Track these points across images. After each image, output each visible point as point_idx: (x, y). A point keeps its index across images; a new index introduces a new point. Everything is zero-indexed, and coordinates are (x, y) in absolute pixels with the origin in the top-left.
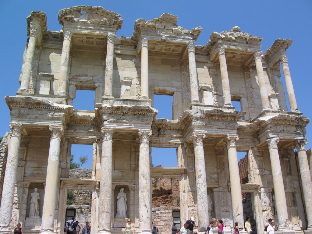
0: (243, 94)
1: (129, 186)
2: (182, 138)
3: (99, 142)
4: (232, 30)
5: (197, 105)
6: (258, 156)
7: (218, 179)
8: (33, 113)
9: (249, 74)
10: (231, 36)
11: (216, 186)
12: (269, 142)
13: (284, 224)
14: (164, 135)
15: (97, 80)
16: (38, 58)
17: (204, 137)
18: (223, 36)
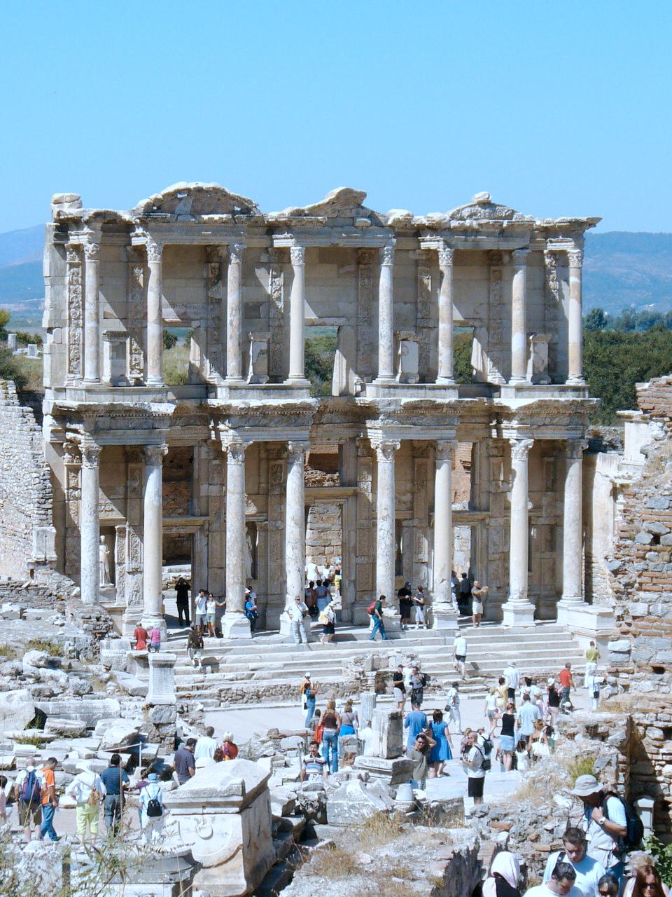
0: (480, 319)
1: (258, 524)
2: (352, 427)
3: (204, 444)
4: (475, 202)
5: (390, 387)
6: (493, 456)
7: (412, 502)
8: (119, 425)
9: (500, 271)
10: (468, 223)
11: (408, 517)
12: (514, 445)
13: (518, 595)
14: (322, 423)
15: (196, 313)
16: (80, 275)
17: (398, 447)
18: (454, 224)
